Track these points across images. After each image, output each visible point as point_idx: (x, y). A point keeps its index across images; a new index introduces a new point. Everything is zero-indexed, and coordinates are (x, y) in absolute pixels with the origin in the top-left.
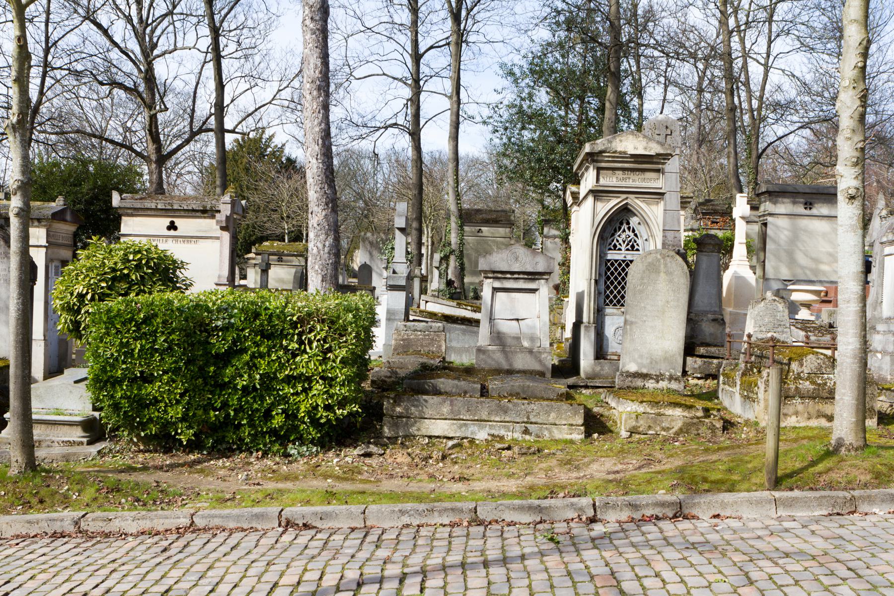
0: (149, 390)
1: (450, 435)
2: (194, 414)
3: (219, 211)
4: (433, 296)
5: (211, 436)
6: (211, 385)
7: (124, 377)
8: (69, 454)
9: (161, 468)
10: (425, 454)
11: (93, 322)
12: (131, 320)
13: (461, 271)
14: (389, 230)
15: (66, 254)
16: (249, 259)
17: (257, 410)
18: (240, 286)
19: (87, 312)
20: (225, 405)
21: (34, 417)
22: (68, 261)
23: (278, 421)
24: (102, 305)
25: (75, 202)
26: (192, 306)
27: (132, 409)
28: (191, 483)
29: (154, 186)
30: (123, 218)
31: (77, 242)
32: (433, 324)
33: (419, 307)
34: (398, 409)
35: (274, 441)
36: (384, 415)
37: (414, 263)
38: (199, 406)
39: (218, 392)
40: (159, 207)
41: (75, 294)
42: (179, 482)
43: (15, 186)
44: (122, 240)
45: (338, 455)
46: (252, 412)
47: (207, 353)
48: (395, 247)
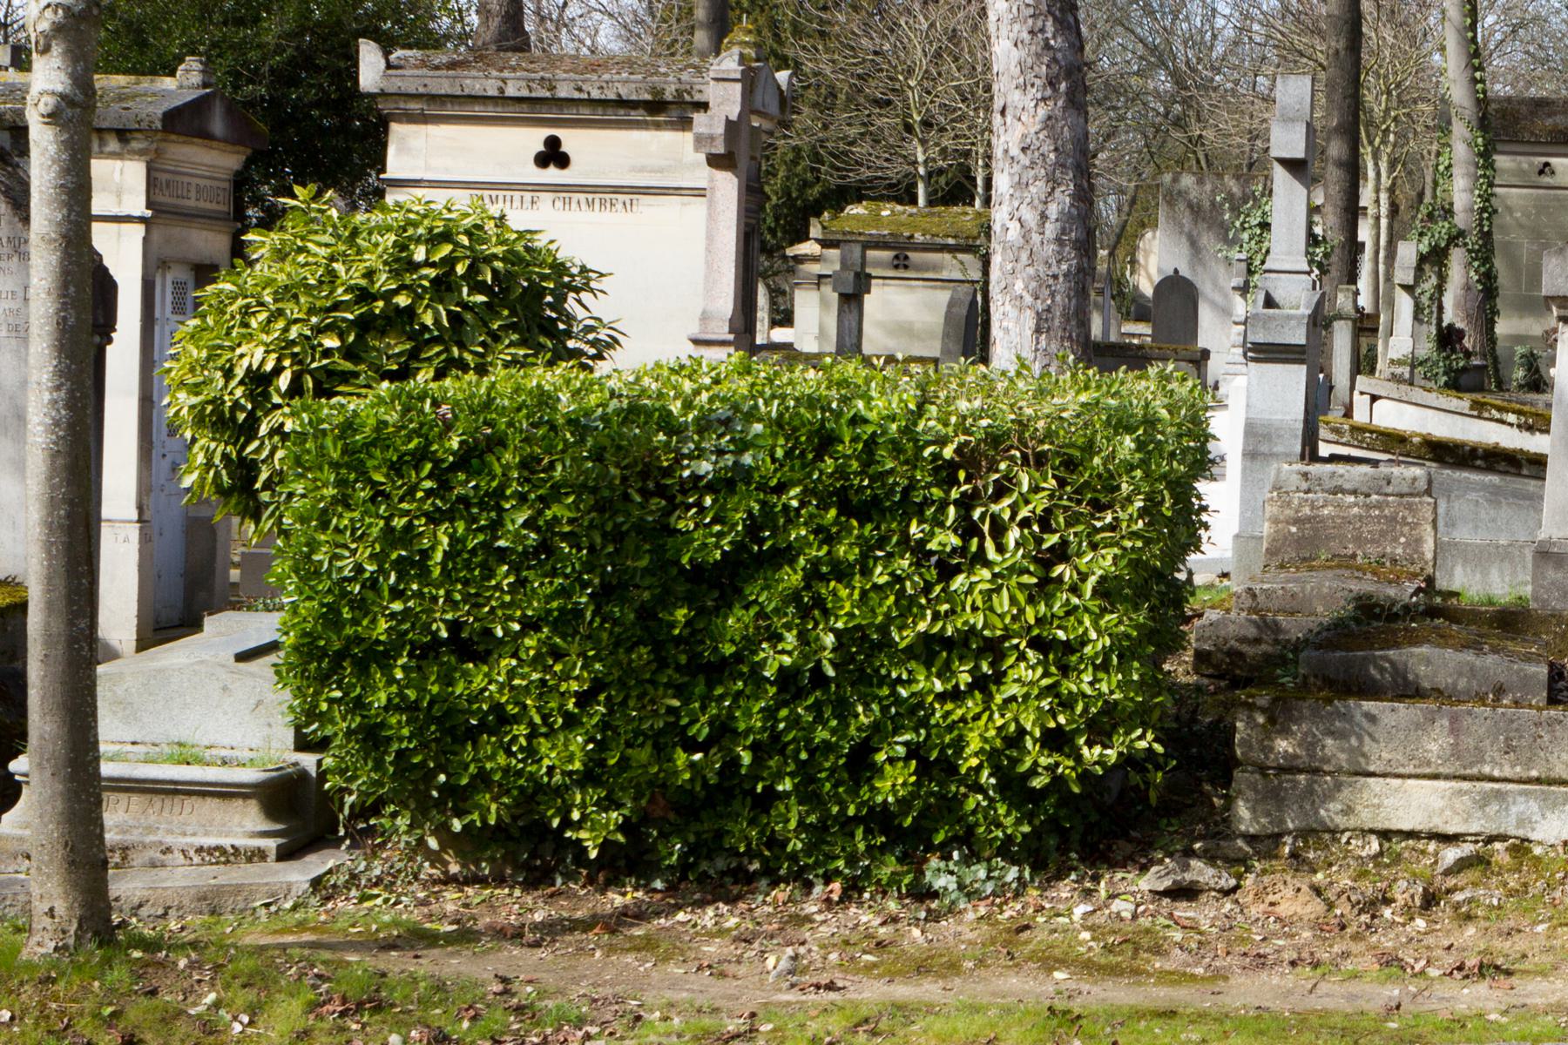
0: (479, 681)
1: (1451, 829)
2: (624, 762)
3: (704, 106)
4: (1395, 378)
5: (679, 831)
6: (678, 668)
7: (397, 641)
8: (219, 891)
9: (515, 935)
10: (1368, 889)
11: (298, 462)
12: (421, 455)
13: (1487, 297)
14: (1254, 167)
15: (210, 243)
16: (799, 259)
17: (827, 747)
18: (773, 347)
19: (278, 430)
20: (724, 731)
21: (107, 769)
22: (215, 268)
23: (893, 782)
24: (328, 409)
25: (237, 75)
26: (618, 412)
27: (424, 745)
28: (613, 984)
29: (495, 23)
30: (395, 128)
31: (247, 205)
32: (1396, 471)
33: (1348, 414)
34: (1283, 745)
35: (883, 849)
36: (1238, 763)
37: (1334, 273)
38: (638, 733)
39: (700, 689)
40: (511, 91)
41: (240, 372)
42: (576, 981)
43: (44, 26)
44: (391, 198)
45: (1088, 894)
46: (811, 753)
47: (664, 563)
48: (1274, 220)
